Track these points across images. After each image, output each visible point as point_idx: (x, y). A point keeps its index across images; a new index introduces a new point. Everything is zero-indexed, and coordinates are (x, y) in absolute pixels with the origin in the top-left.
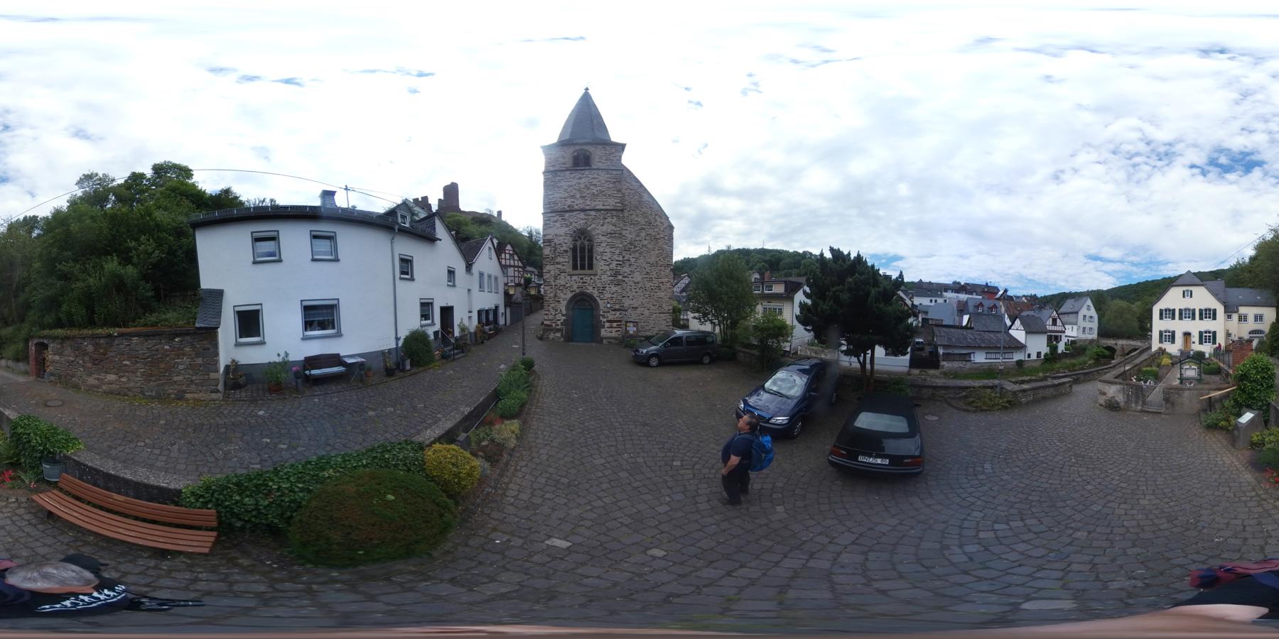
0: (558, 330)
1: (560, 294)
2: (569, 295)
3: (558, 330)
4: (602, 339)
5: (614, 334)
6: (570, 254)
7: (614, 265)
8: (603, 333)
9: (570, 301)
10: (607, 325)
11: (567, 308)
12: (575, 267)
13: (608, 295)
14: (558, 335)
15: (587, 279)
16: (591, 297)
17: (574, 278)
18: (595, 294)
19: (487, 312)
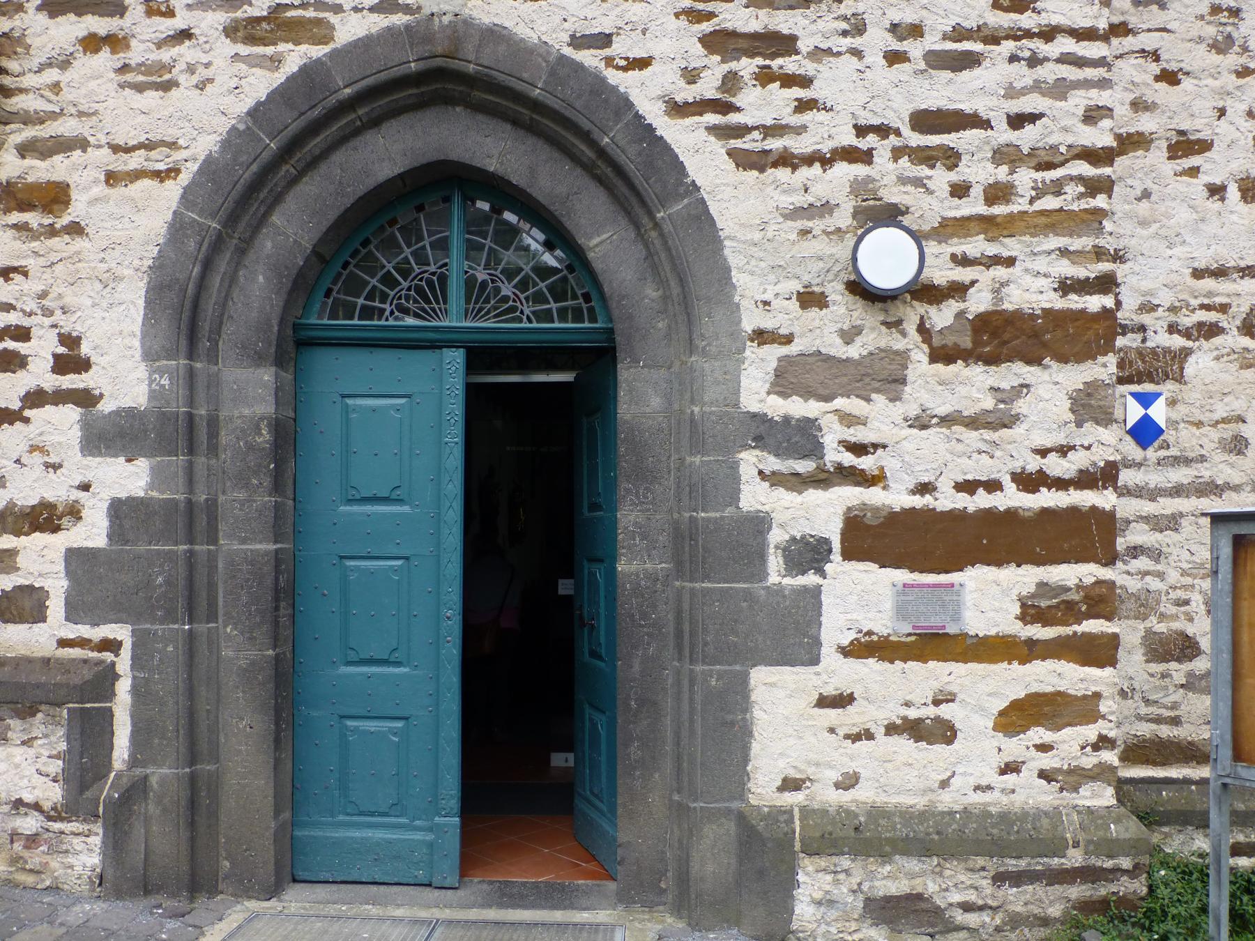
4: (768, 853)
5: (977, 770)
8: (799, 736)
10: (861, 596)
11: (186, 314)
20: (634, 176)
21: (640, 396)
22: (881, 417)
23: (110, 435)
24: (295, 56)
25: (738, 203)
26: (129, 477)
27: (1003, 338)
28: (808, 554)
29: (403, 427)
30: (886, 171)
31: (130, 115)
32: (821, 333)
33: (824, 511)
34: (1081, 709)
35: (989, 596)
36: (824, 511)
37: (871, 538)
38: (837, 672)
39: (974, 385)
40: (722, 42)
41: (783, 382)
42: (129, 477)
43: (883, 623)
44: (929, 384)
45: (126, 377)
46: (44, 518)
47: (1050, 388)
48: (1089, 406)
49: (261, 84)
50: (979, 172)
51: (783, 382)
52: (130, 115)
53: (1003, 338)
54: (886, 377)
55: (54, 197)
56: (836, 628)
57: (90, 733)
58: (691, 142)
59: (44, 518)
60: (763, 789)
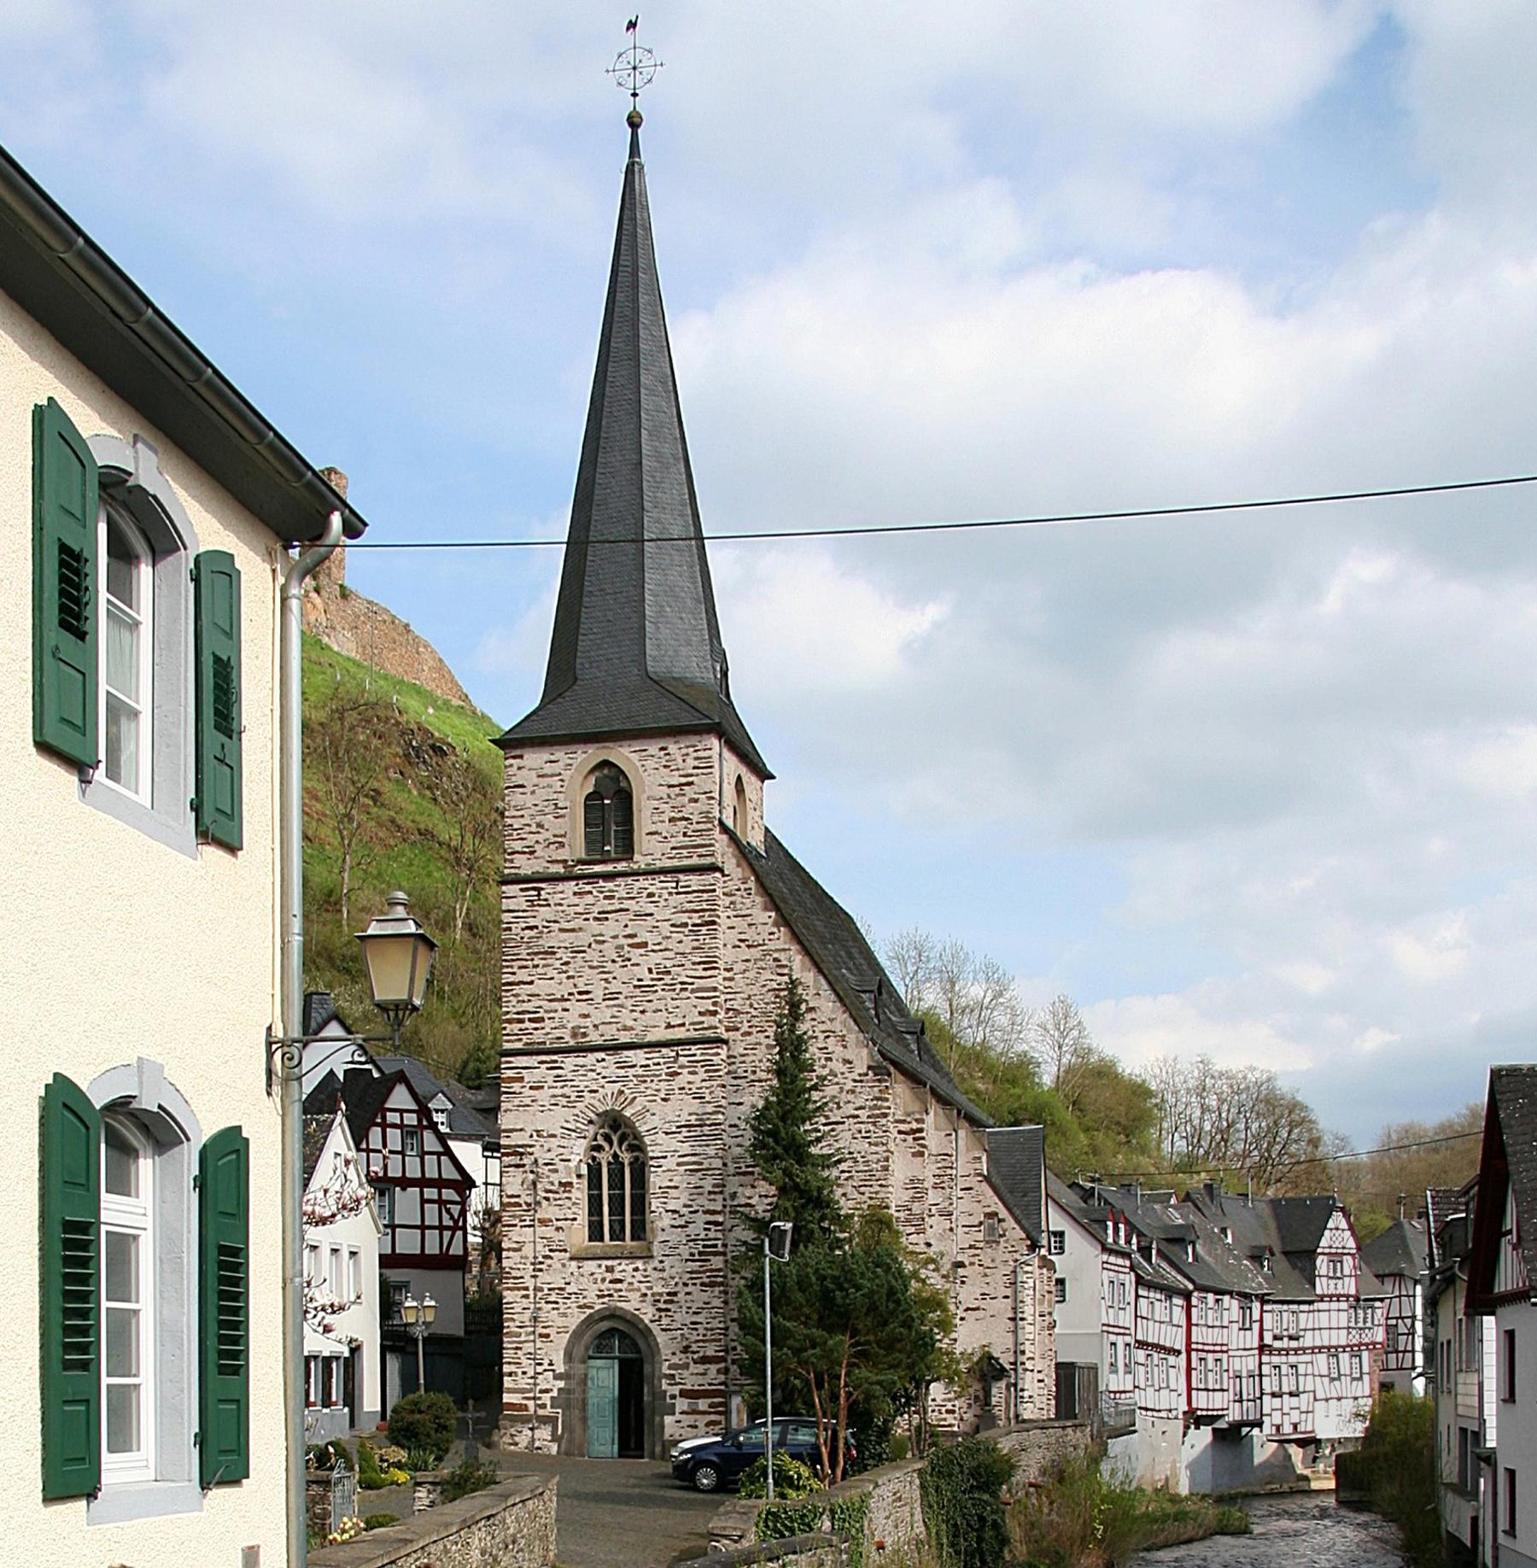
0: (544, 1420)
1: (548, 1314)
2: (576, 1318)
3: (544, 1420)
6: (580, 1193)
7: (697, 1229)
9: (577, 1335)
10: (682, 1404)
11: (569, 1356)
12: (595, 1233)
13: (681, 1317)
14: (544, 1433)
15: (624, 1268)
16: (632, 1321)
17: (590, 1266)
18: (647, 1314)
19: (327, 1361)
20: (647, 1333)
21: (647, 1369)
22: (686, 1373)
23: (557, 1377)
24: (589, 1311)
25: (661, 1338)
26: (561, 1384)
27: (705, 1360)
28: (673, 1397)
29: (605, 1378)
30: (686, 1331)
31: (560, 1322)
32: (675, 1360)
33: (676, 1390)
34: (719, 1423)
35: (703, 1404)
36: (676, 1390)
37: (683, 1394)
38: (678, 1417)
39: (701, 1368)
40: (659, 1310)
41: (670, 1368)
42: (561, 1384)
43: (685, 1408)
44: (693, 1368)
45: (560, 1368)
46: (547, 1391)
47: (713, 1368)
48: (719, 1371)
49: (583, 1317)
50: (701, 1331)
51: (670, 1368)
52: (560, 1322)
53: (705, 1360)
54: (686, 1366)
55: (548, 1336)
56: (678, 1410)
57: (555, 1428)
58: (654, 1328)
59: (547, 1391)
60: (667, 1436)
